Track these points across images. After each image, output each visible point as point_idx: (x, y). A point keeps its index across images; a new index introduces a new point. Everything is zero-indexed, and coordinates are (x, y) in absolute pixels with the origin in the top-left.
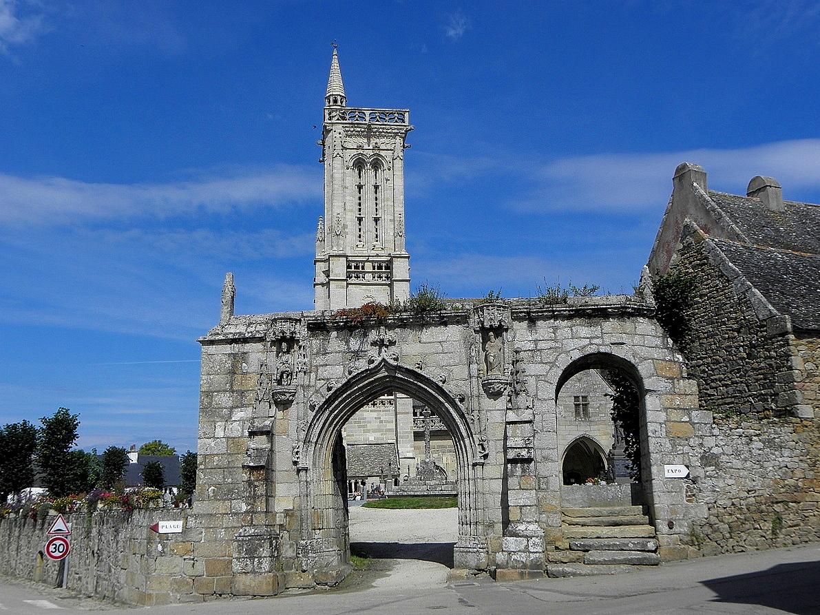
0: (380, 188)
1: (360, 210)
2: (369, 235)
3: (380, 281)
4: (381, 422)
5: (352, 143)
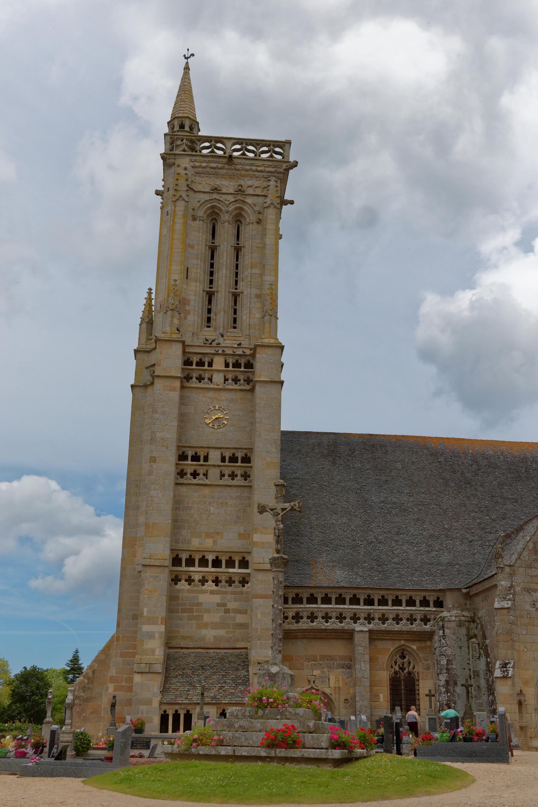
1: (211, 282)
2: (221, 317)
3: (237, 387)
4: (227, 611)
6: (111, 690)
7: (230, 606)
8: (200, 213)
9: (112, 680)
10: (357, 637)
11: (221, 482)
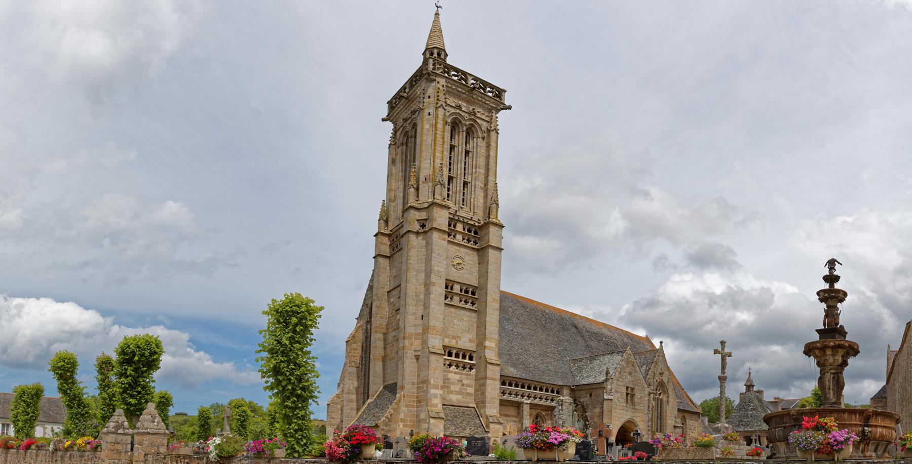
0: (470, 154)
4: (463, 385)
5: (452, 101)
6: (401, 426)
7: (465, 382)
8: (449, 120)
9: (402, 420)
10: (525, 406)
11: (460, 305)
